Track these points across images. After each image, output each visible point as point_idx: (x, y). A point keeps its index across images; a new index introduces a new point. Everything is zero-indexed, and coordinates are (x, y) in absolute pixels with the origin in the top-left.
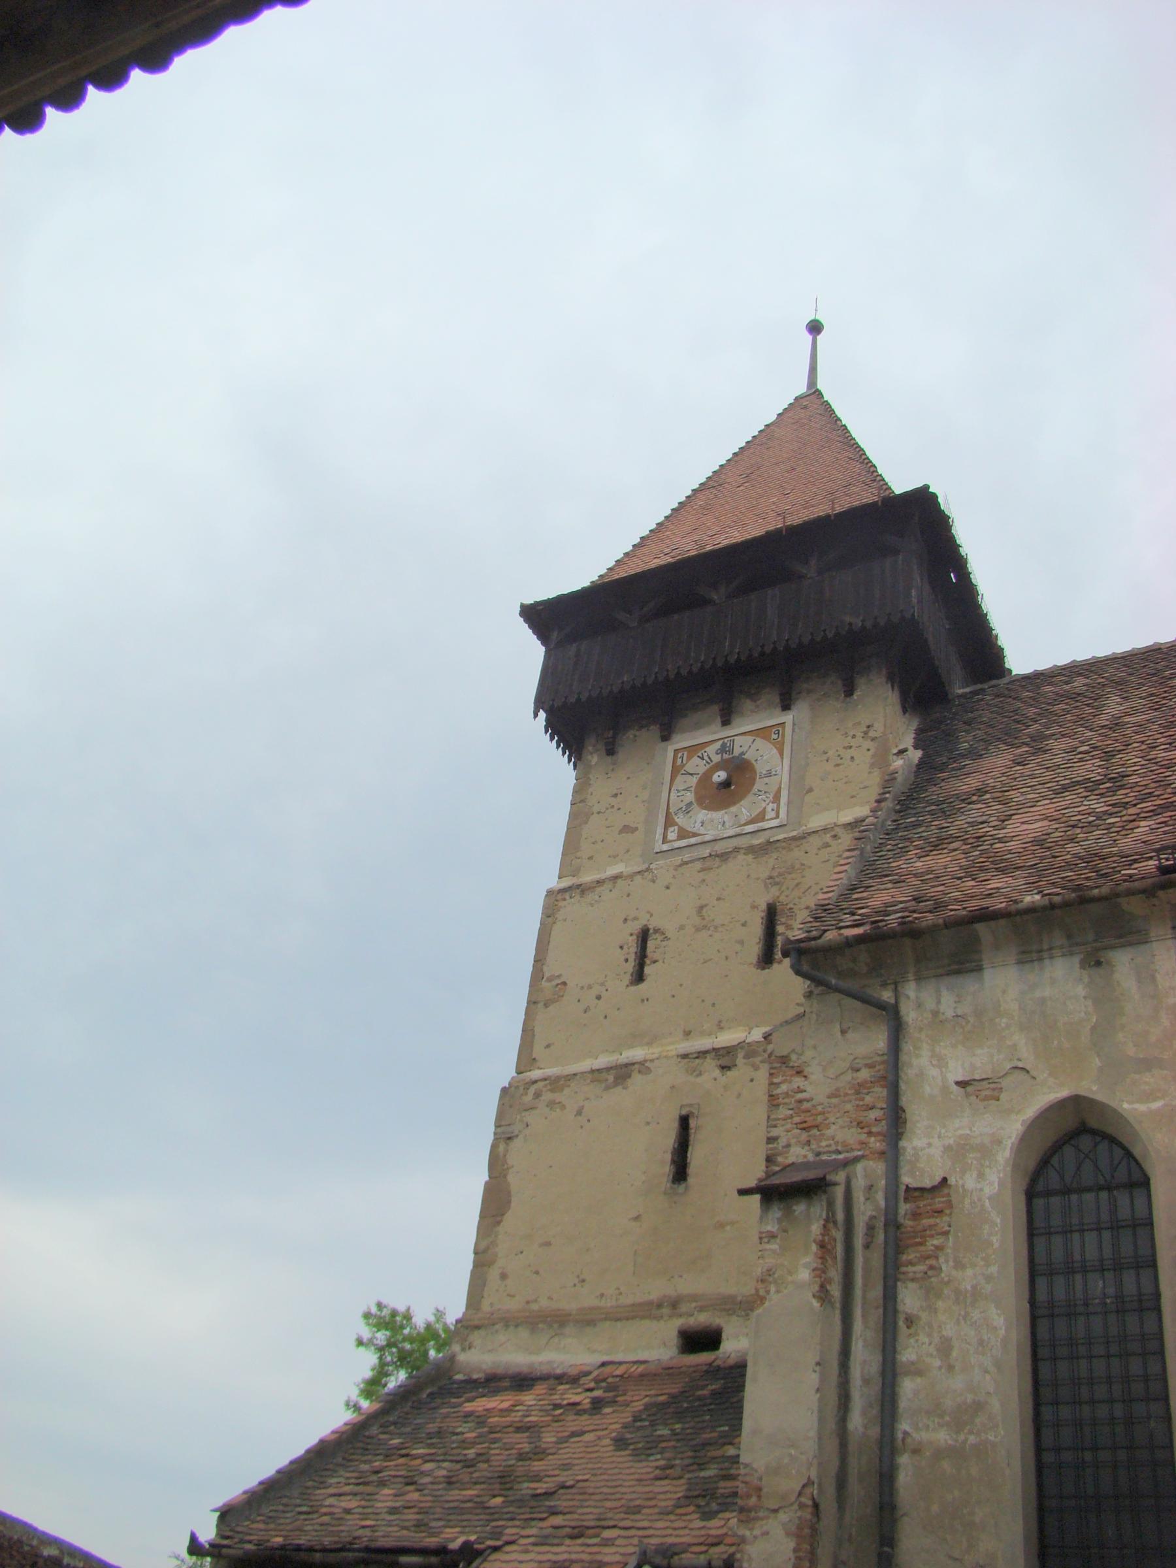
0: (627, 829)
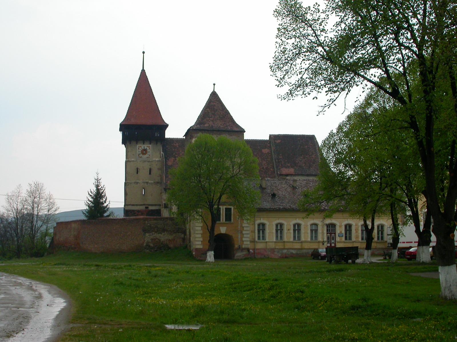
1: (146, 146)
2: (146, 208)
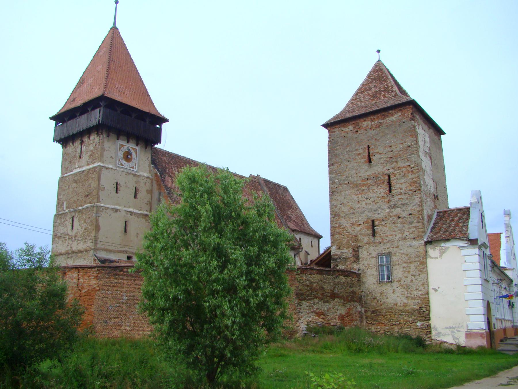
0: (111, 157)
1: (131, 146)
2: (129, 258)
